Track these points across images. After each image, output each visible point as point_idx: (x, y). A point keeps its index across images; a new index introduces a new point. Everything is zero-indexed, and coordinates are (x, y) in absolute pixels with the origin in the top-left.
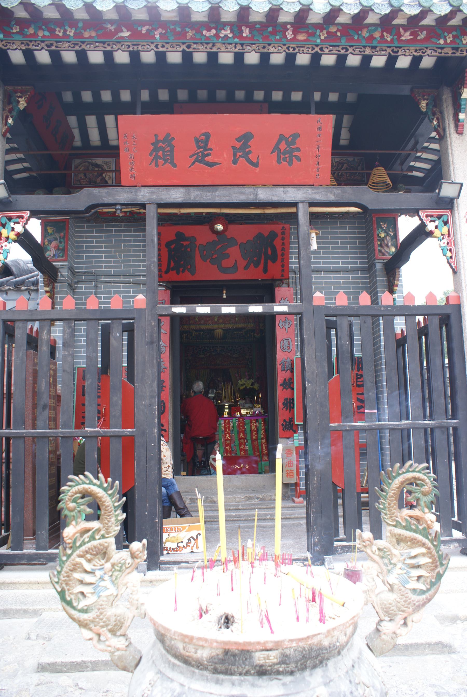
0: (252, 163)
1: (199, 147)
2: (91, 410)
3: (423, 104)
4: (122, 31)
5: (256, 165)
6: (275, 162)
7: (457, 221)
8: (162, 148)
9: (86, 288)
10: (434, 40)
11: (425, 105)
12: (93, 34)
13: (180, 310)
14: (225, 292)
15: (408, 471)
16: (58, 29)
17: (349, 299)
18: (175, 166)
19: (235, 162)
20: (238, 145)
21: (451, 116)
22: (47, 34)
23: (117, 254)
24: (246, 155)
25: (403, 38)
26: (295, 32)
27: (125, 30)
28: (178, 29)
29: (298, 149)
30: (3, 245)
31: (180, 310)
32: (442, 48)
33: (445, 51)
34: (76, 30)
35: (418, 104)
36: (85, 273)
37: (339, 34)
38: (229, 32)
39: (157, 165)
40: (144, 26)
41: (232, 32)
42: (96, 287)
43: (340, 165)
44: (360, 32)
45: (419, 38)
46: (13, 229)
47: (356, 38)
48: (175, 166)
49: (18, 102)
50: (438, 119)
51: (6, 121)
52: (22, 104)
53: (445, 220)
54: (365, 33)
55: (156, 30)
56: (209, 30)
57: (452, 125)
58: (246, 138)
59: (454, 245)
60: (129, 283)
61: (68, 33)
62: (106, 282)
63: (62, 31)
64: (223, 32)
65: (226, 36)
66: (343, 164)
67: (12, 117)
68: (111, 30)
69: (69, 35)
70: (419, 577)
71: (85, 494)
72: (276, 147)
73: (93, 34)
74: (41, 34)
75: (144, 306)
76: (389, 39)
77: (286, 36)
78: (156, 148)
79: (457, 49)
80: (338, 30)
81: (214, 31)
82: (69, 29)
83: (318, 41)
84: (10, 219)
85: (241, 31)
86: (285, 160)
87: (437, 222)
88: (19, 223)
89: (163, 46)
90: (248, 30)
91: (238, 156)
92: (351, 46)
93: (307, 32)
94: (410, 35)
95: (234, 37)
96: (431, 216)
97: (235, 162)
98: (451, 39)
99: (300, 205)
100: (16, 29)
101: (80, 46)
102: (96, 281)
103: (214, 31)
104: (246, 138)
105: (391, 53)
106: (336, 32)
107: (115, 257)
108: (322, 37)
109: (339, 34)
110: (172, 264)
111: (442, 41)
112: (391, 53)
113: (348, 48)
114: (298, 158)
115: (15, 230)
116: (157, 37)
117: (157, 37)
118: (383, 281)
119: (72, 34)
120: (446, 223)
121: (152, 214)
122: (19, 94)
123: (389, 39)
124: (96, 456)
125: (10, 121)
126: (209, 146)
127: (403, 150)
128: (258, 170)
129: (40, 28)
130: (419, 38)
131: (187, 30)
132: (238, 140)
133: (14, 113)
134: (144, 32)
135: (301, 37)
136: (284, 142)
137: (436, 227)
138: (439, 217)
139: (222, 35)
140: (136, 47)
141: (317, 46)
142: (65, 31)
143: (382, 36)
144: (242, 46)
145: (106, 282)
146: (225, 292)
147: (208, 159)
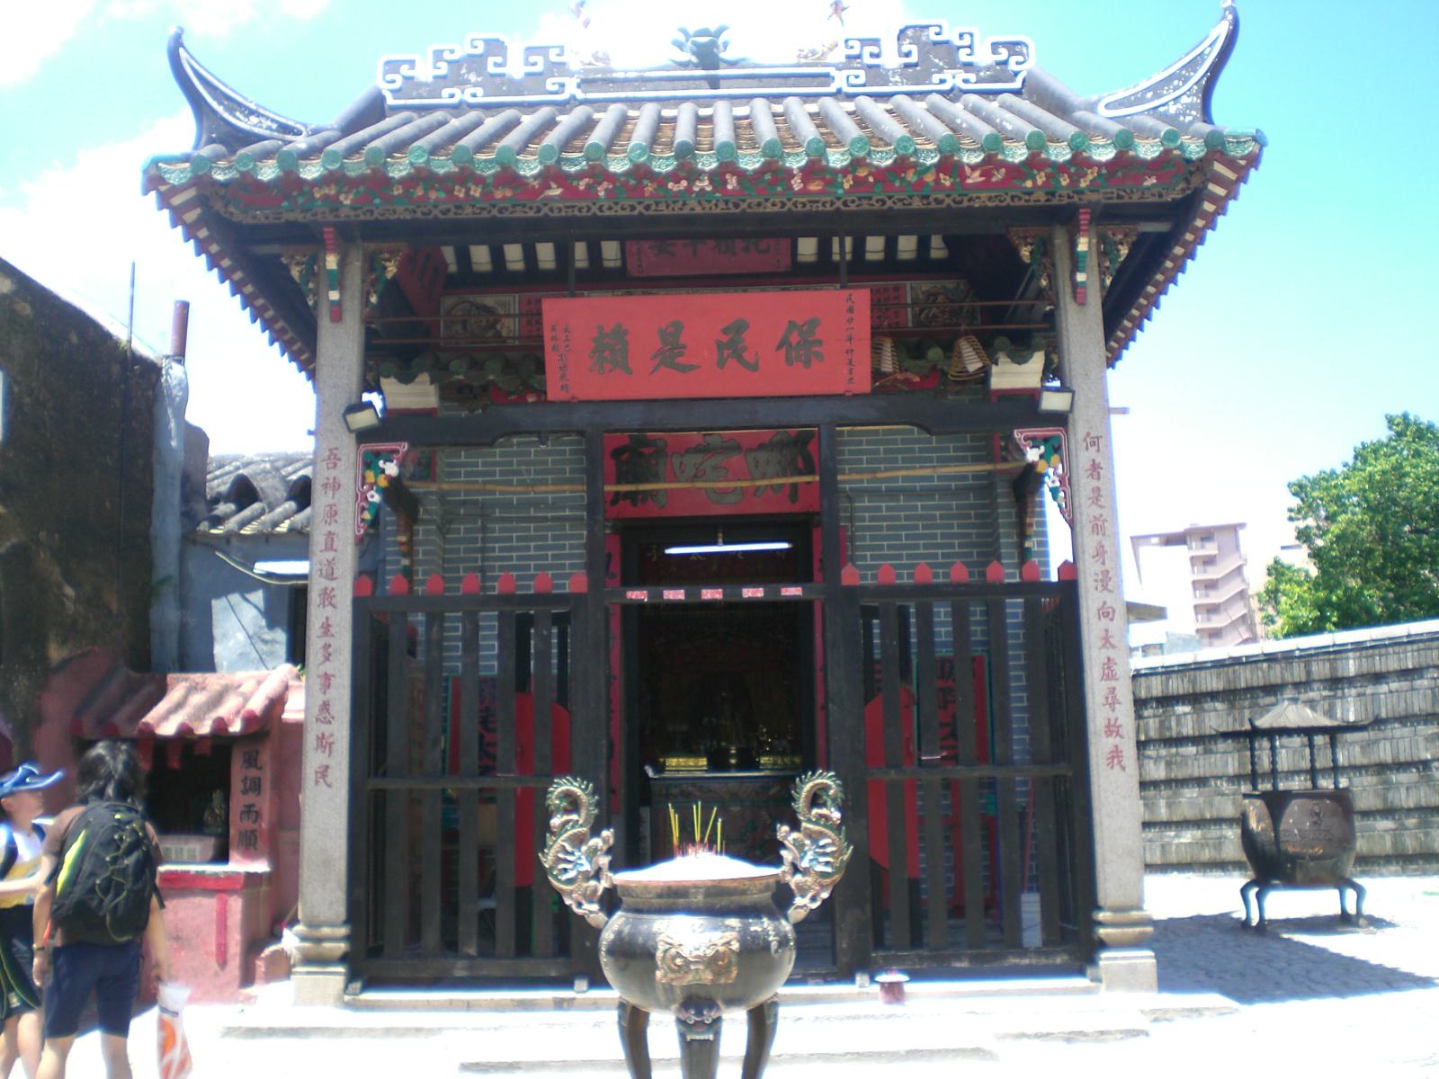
2: (505, 746)
3: (1025, 252)
4: (550, 188)
7: (1072, 447)
9: (467, 530)
10: (1016, 182)
11: (1027, 254)
12: (509, 193)
13: (638, 595)
14: (720, 535)
15: (817, 778)
16: (457, 188)
19: (721, 364)
20: (725, 339)
21: (1067, 275)
22: (442, 195)
23: (523, 468)
25: (969, 181)
26: (805, 180)
27: (554, 185)
28: (632, 182)
30: (368, 495)
31: (638, 595)
32: (1029, 194)
34: (483, 189)
35: (1015, 253)
36: (464, 503)
37: (871, 179)
38: (707, 183)
40: (582, 179)
41: (711, 182)
42: (484, 529)
43: (932, 298)
44: (903, 175)
45: (994, 179)
46: (383, 471)
47: (897, 184)
49: (385, 268)
50: (1049, 277)
51: (368, 300)
52: (392, 269)
53: (1056, 446)
54: (911, 177)
55: (600, 184)
56: (677, 182)
57: (1068, 290)
58: (738, 328)
59: (1070, 484)
60: (545, 519)
61: (472, 193)
62: (503, 520)
63: (463, 190)
64: (698, 183)
65: (702, 190)
66: (936, 295)
67: (375, 292)
68: (534, 186)
69: (473, 197)
70: (827, 863)
73: (509, 193)
74: (433, 195)
76: (948, 184)
77: (790, 187)
80: (870, 174)
81: (684, 183)
82: (473, 188)
83: (840, 191)
84: (378, 455)
85: (725, 182)
87: (1042, 448)
88: (391, 461)
89: (610, 208)
90: (734, 180)
91: (725, 356)
92: (890, 198)
93: (823, 179)
94: (981, 176)
96: (1033, 439)
97: (721, 364)
98: (1044, 179)
99: (822, 427)
100: (398, 189)
101: (490, 212)
102: (484, 516)
103: (684, 183)
104: (738, 328)
105: (952, 204)
106: (867, 176)
107: (519, 473)
108: (847, 186)
109: (871, 179)
112: (952, 204)
113: (887, 199)
115: (387, 472)
116: (602, 194)
117: (602, 194)
118: (1009, 515)
119: (477, 195)
120: (1057, 450)
122: (387, 256)
123: (948, 184)
124: (513, 816)
127: (1021, 298)
129: (432, 188)
130: (994, 179)
131: (645, 182)
132: (725, 331)
133: (380, 287)
134: (582, 188)
136: (796, 333)
137: (1041, 457)
138: (1046, 440)
139: (696, 189)
140: (570, 210)
141: (838, 199)
142: (468, 190)
143: (937, 180)
144: (727, 204)
145: (503, 520)
146: (720, 535)
147: (680, 360)
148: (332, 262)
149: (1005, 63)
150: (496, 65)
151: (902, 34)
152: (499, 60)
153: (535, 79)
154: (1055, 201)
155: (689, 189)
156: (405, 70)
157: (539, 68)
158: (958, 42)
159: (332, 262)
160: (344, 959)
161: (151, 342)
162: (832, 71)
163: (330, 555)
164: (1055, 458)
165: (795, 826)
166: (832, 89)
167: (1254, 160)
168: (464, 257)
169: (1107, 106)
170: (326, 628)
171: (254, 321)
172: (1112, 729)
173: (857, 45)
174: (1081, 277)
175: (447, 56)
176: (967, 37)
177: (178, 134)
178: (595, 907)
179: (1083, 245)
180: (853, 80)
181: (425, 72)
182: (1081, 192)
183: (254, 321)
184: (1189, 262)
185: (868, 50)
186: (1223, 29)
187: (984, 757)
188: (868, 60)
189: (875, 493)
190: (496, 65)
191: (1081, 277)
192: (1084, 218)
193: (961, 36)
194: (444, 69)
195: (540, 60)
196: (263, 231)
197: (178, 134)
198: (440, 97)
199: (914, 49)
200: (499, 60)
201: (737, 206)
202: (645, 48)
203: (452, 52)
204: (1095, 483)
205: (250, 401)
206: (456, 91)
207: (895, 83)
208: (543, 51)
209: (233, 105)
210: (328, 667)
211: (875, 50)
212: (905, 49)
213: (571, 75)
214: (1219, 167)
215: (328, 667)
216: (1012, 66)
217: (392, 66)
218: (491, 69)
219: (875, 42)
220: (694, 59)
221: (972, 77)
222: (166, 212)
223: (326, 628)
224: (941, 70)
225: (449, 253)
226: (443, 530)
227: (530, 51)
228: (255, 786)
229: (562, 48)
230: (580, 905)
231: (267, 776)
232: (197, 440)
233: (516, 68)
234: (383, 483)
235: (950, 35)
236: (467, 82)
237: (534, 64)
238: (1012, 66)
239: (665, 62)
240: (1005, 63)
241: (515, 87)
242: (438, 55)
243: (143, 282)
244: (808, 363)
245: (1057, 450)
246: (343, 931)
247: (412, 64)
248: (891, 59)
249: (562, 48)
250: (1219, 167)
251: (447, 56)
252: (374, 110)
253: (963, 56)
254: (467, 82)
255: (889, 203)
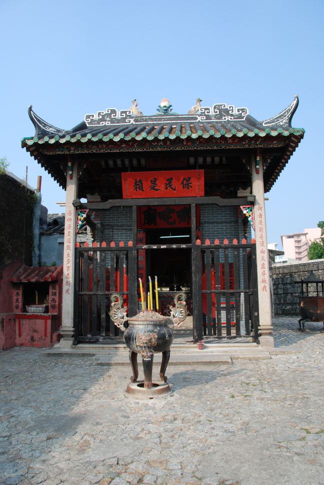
0: (173, 189)
1: (152, 184)
3: (244, 161)
4: (122, 145)
5: (175, 190)
6: (182, 189)
8: (138, 184)
9: (108, 232)
17: (210, 241)
18: (143, 191)
19: (166, 189)
21: (254, 166)
24: (170, 186)
26: (187, 142)
28: (143, 143)
29: (191, 183)
33: (246, 146)
36: (107, 225)
39: (136, 191)
41: (163, 142)
42: (112, 231)
48: (143, 191)
55: (135, 143)
56: (155, 143)
57: (255, 170)
65: (161, 145)
71: (115, 297)
72: (182, 183)
75: (132, 246)
78: (136, 185)
79: (250, 145)
85: (167, 143)
86: (186, 187)
95: (164, 145)
97: (166, 189)
102: (113, 229)
110: (146, 221)
111: (244, 143)
114: (191, 187)
120: (251, 210)
121: (134, 208)
125: (80, 173)
126: (156, 183)
128: (175, 192)
135: (189, 144)
137: (247, 212)
138: (248, 208)
148: (70, 164)
149: (241, 114)
150: (114, 116)
151: (215, 108)
152: (114, 115)
153: (123, 120)
154: (251, 147)
155: (157, 144)
156: (91, 117)
157: (124, 116)
158: (229, 109)
159: (70, 164)
160: (73, 336)
161: (32, 185)
162: (197, 116)
163: (69, 237)
164: (251, 213)
165: (174, 306)
166: (197, 121)
167: (302, 136)
168: (107, 163)
169: (265, 124)
170: (68, 255)
171: (55, 180)
172: (68, 283)
173: (203, 110)
174: (258, 167)
175: (102, 114)
176: (231, 108)
177: (30, 132)
178: (122, 326)
179: (258, 159)
180: (202, 119)
181: (96, 117)
182: (257, 145)
183: (55, 180)
184: (286, 164)
185: (206, 111)
186: (295, 102)
187: (231, 287)
188: (206, 114)
189: (209, 223)
190: (114, 116)
191: (258, 167)
192: (258, 151)
193: (230, 107)
194: (101, 117)
195: (124, 114)
196: (52, 154)
197: (30, 132)
198: (100, 124)
199: (218, 111)
200: (114, 115)
201: (170, 149)
202: (150, 110)
203: (103, 113)
204: (260, 219)
205: (57, 199)
206: (104, 123)
207: (213, 119)
208: (125, 112)
209: (45, 125)
210: (69, 265)
211: (208, 111)
212: (216, 111)
213: (132, 118)
214: (293, 139)
215: (69, 265)
216: (243, 115)
217: (88, 117)
218: (112, 117)
219: (208, 109)
220: (163, 114)
221: (233, 118)
222: (29, 153)
223: (68, 255)
224: (225, 116)
225: (103, 163)
226: (102, 232)
227: (122, 112)
228: (55, 294)
229: (130, 111)
230: (119, 325)
231: (57, 291)
232: (45, 210)
233: (118, 116)
234: (82, 218)
235: (227, 107)
236: (106, 120)
237: (123, 115)
238: (243, 115)
239: (155, 114)
240: (241, 114)
241: (119, 121)
242: (99, 114)
243: (29, 172)
244: (188, 189)
245: (251, 210)
246: (72, 329)
247: (93, 116)
248: (212, 113)
249: (130, 111)
250: (293, 139)
251: (102, 114)
252: (82, 127)
253: (230, 112)
254: (106, 120)
255: (208, 148)
